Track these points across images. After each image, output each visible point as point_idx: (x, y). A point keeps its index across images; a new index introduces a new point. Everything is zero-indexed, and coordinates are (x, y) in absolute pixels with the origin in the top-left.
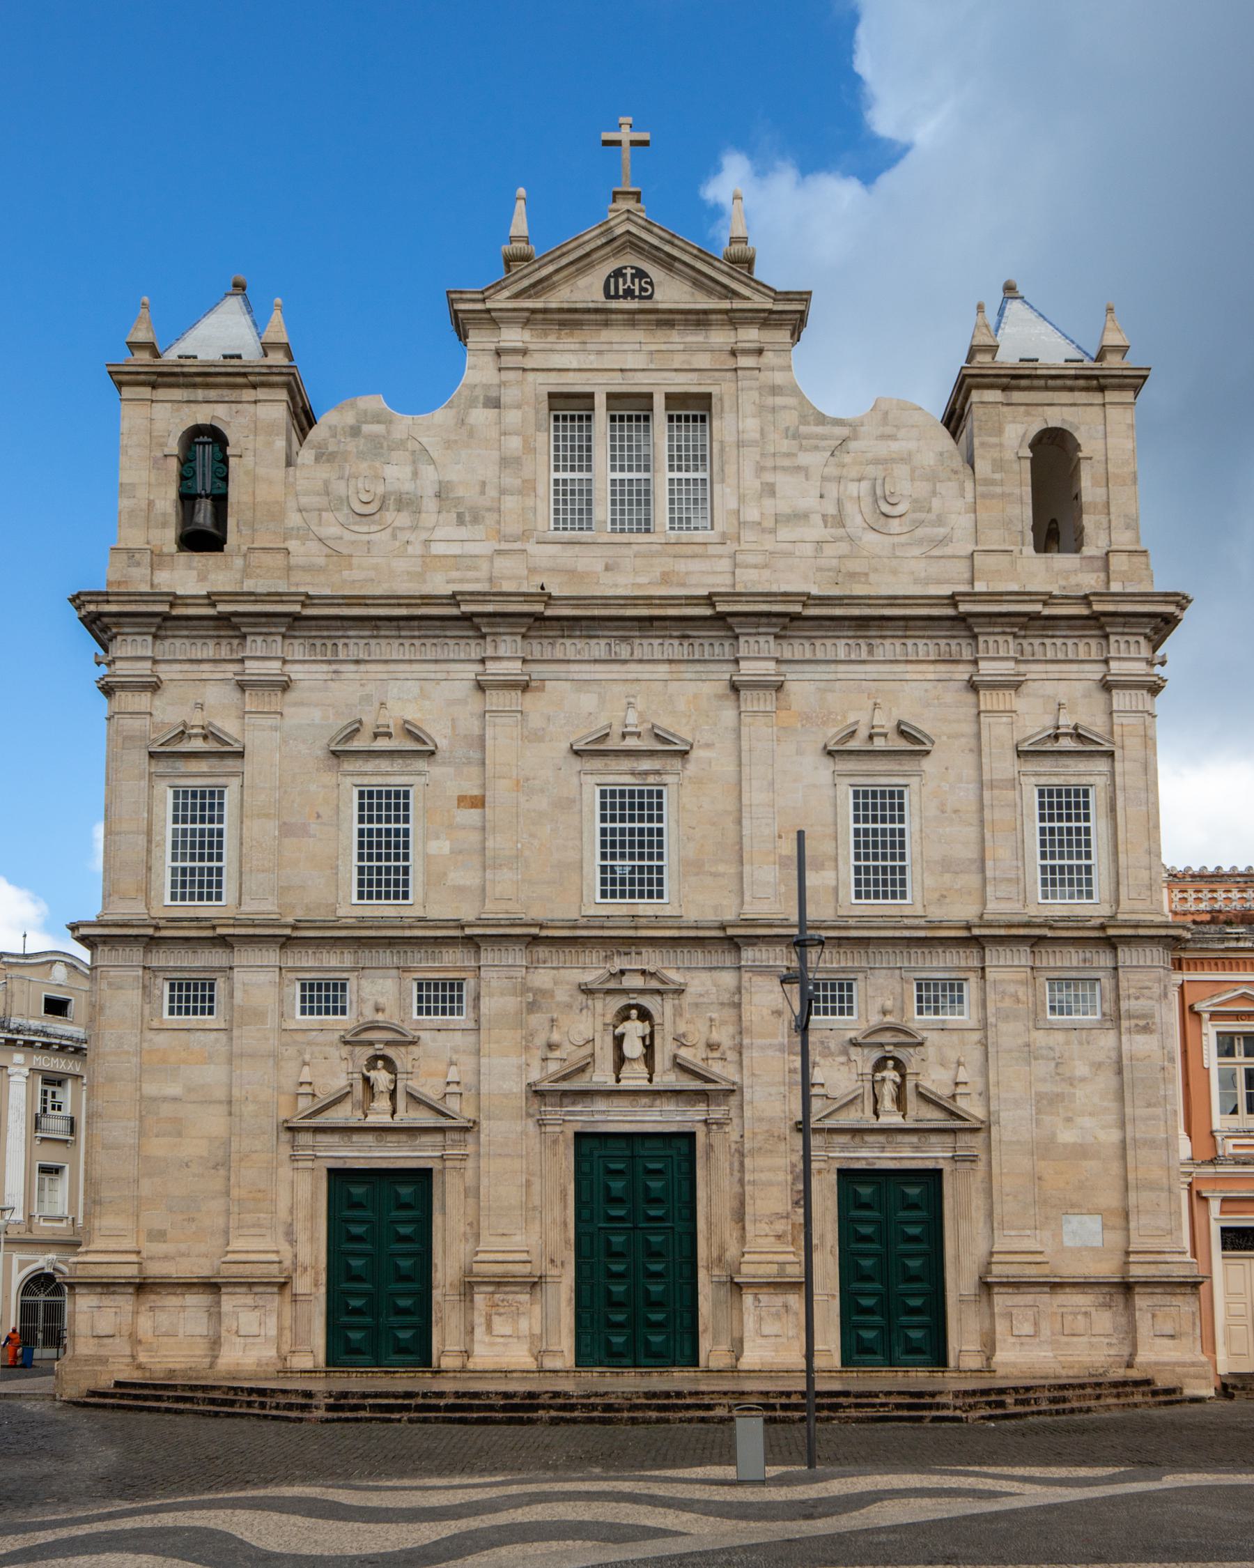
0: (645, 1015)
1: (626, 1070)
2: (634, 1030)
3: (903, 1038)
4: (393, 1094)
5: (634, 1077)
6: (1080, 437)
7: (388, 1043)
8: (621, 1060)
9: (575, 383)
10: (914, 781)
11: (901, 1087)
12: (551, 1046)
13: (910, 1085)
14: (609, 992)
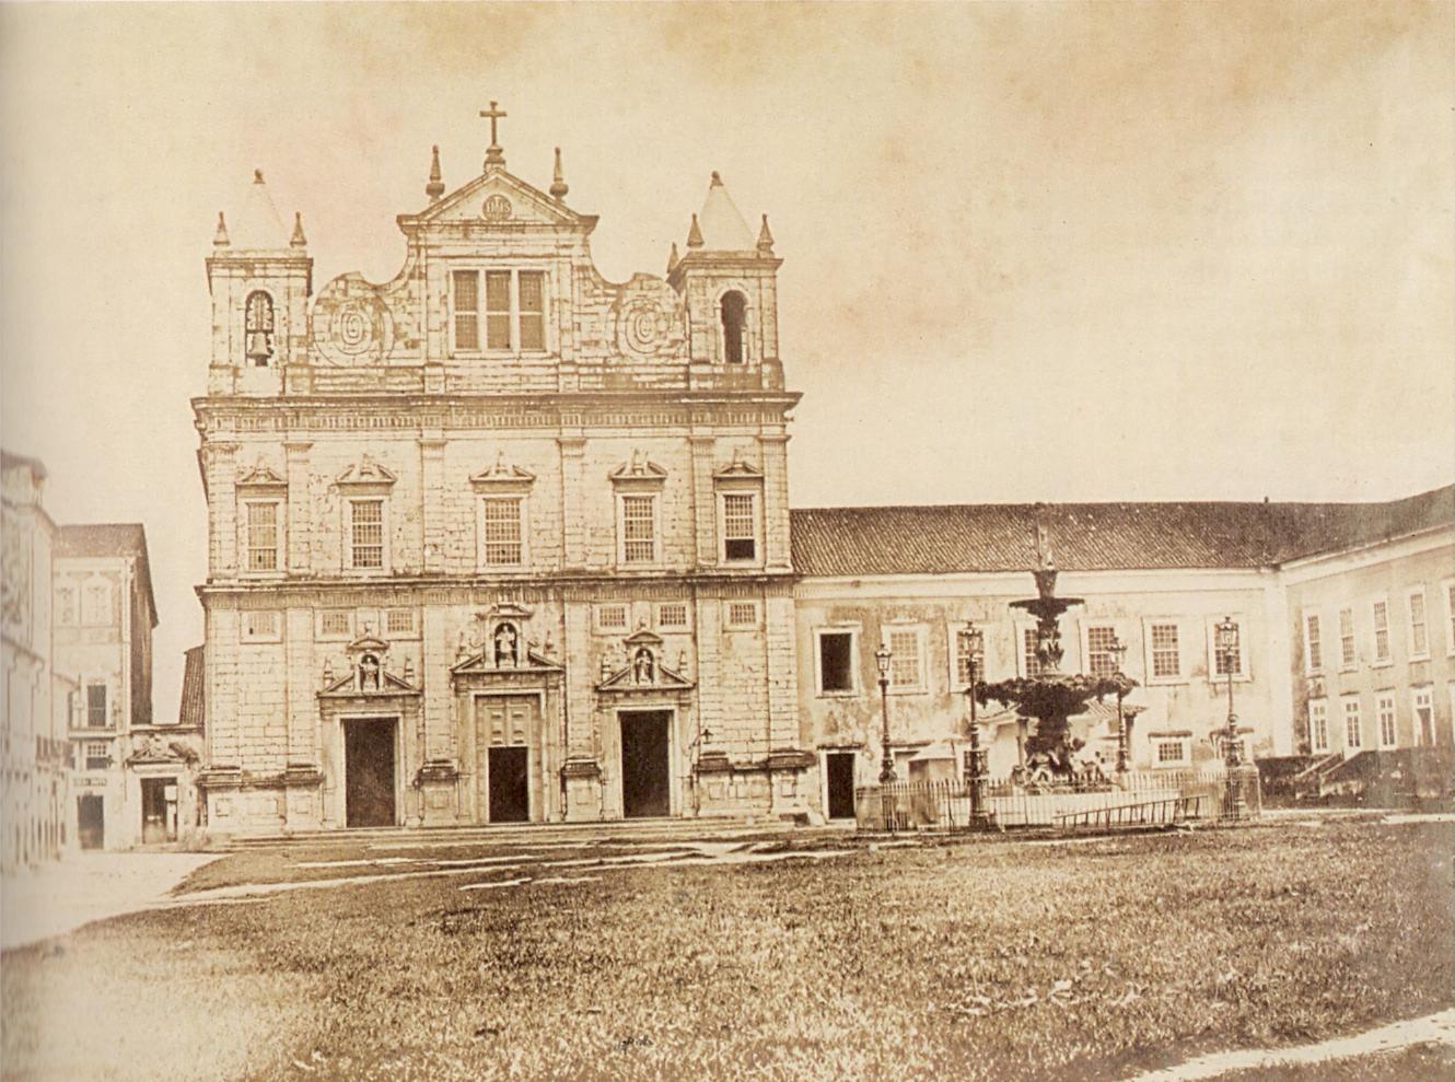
0: (511, 629)
1: (502, 662)
2: (507, 636)
3: (651, 639)
4: (376, 677)
5: (507, 665)
6: (747, 296)
7: (374, 649)
8: (499, 656)
9: (472, 265)
10: (658, 494)
11: (650, 667)
12: (462, 648)
13: (655, 664)
14: (493, 617)
